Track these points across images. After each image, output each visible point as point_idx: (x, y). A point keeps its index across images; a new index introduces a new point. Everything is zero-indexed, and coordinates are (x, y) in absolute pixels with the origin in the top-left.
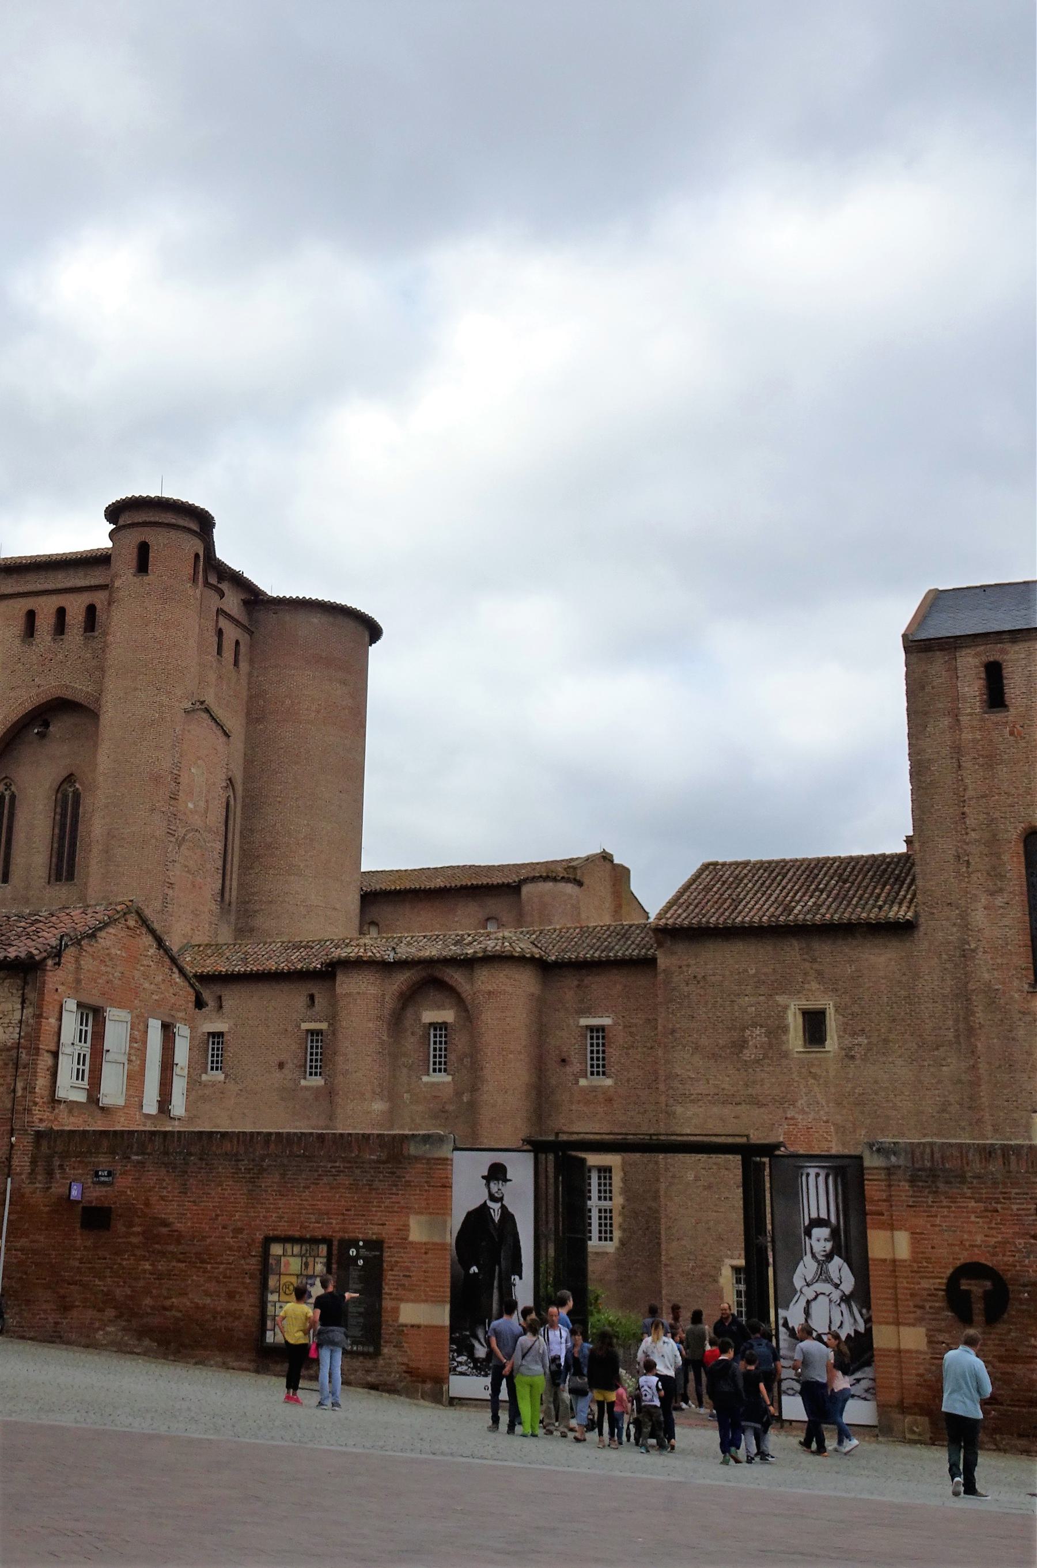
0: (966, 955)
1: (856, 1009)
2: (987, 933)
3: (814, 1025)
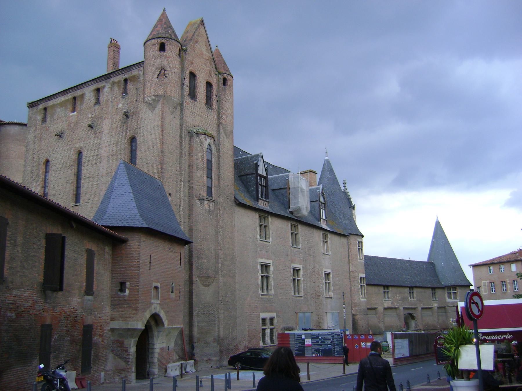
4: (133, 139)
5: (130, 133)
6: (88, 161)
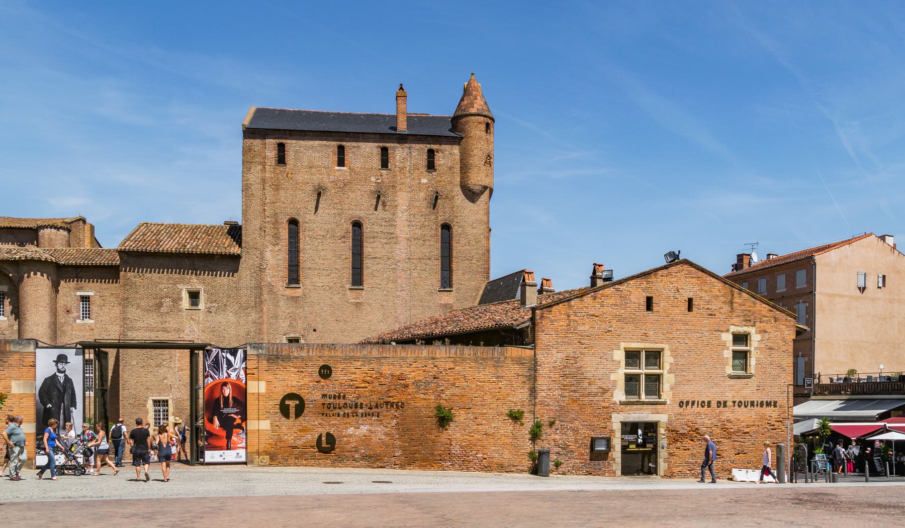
0: (261, 270)
1: (213, 291)
2: (271, 262)
3: (194, 296)
4: (446, 227)
5: (441, 219)
6: (374, 238)
